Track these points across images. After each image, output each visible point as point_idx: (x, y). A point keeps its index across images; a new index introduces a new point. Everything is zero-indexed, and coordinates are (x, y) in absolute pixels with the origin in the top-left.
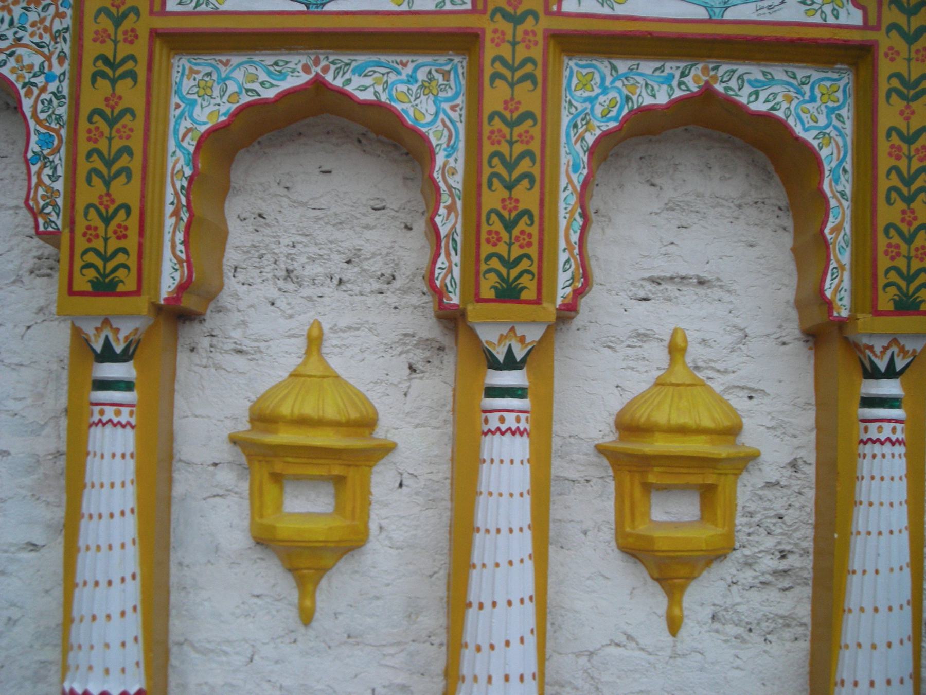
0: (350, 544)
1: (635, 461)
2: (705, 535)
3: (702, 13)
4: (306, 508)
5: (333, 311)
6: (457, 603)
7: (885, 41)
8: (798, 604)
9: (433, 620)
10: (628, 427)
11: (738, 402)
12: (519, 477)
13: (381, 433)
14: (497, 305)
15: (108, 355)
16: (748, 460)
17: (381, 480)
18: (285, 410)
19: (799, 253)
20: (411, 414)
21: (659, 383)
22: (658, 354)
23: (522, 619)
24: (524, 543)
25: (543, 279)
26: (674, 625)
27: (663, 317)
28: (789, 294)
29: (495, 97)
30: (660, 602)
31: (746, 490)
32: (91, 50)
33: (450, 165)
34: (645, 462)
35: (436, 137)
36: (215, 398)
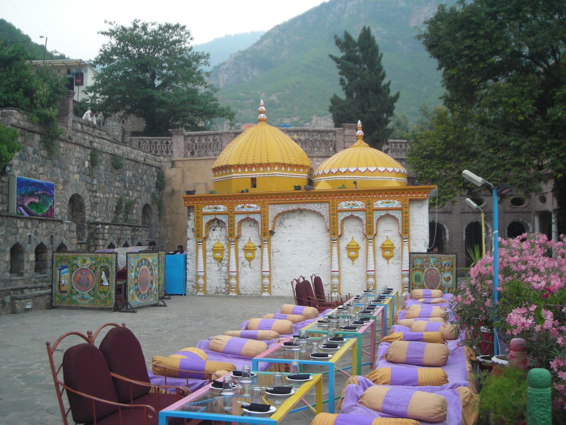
0: (357, 257)
1: (384, 248)
4: (353, 254)
5: (354, 235)
6: (367, 262)
9: (365, 264)
10: (383, 245)
12: (372, 250)
14: (370, 233)
17: (360, 251)
22: (385, 238)
23: (373, 262)
24: (372, 256)
25: (373, 232)
26: (388, 264)
27: (386, 234)
30: (387, 261)
31: (395, 250)
33: (364, 222)
36: (344, 244)
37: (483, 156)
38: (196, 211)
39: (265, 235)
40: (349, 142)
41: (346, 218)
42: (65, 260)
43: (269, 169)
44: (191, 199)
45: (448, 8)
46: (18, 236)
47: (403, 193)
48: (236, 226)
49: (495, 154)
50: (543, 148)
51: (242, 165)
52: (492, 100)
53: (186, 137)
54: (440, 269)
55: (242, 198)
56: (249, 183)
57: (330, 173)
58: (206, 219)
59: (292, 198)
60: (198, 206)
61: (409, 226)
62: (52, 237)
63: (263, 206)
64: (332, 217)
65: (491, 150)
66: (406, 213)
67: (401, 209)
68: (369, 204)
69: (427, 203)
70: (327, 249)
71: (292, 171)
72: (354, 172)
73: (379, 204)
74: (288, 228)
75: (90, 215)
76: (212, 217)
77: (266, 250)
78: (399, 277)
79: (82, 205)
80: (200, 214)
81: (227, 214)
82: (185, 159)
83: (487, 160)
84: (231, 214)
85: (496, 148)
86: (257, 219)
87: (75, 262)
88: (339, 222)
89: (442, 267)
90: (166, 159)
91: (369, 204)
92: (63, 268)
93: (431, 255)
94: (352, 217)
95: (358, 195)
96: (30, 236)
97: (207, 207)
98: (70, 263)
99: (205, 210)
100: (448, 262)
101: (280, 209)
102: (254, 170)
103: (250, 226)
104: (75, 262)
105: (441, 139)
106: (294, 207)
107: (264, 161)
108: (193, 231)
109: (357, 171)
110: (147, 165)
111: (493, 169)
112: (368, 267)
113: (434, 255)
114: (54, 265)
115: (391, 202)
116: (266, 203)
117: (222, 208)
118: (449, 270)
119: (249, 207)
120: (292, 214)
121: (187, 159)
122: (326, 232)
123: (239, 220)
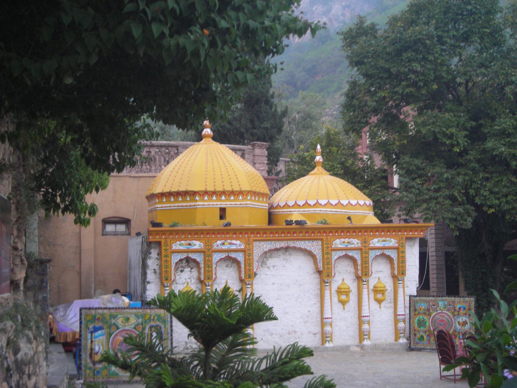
0: (348, 301)
1: (376, 291)
2: (383, 298)
3: (382, 245)
4: (343, 297)
5: (345, 276)
7: (400, 247)
8: (392, 305)
9: (357, 309)
10: (375, 287)
11: (385, 284)
13: (351, 289)
15: (328, 283)
16: (387, 290)
17: (351, 294)
18: (343, 287)
19: (391, 267)
20: (353, 286)
21: (377, 282)
26: (380, 308)
27: (377, 275)
28: (390, 272)
29: (364, 255)
30: (378, 305)
31: (386, 293)
32: (325, 251)
33: (359, 262)
34: (377, 291)
35: (358, 259)
36: (335, 287)
37: (413, 187)
38: (163, 248)
39: (250, 277)
40: (259, 163)
41: (340, 257)
42: (98, 319)
43: (241, 198)
44: (157, 233)
45: (368, 23)
47: (400, 231)
48: (214, 266)
49: (423, 184)
50: (474, 181)
51: (210, 191)
52: (432, 129)
54: (453, 313)
55: (223, 233)
56: (218, 214)
57: (306, 204)
58: (175, 258)
59: (281, 233)
60: (166, 241)
61: (405, 266)
63: (248, 243)
65: (418, 181)
66: (404, 252)
67: (397, 248)
68: (365, 242)
69: (418, 241)
70: (316, 292)
72: (336, 205)
73: (376, 242)
74: (271, 268)
76: (184, 256)
78: (391, 322)
80: (170, 251)
81: (204, 252)
83: (417, 191)
84: (207, 253)
85: (423, 179)
86: (239, 259)
87: (113, 321)
88: (333, 262)
89: (455, 310)
91: (365, 242)
92: (96, 330)
93: (440, 298)
94: (346, 257)
95: (354, 232)
97: (178, 242)
98: (107, 323)
99: (176, 246)
100: (466, 305)
101: (267, 246)
102: (223, 198)
103: (227, 266)
104: (113, 321)
105: (338, 164)
106: (283, 244)
107: (236, 188)
108: (155, 272)
109: (339, 205)
111: (425, 201)
112: (363, 312)
113: (444, 298)
114: (83, 326)
115: (388, 241)
116: (251, 239)
117: (197, 245)
118: (466, 314)
119: (230, 244)
120: (276, 252)
122: (314, 273)
123: (218, 259)
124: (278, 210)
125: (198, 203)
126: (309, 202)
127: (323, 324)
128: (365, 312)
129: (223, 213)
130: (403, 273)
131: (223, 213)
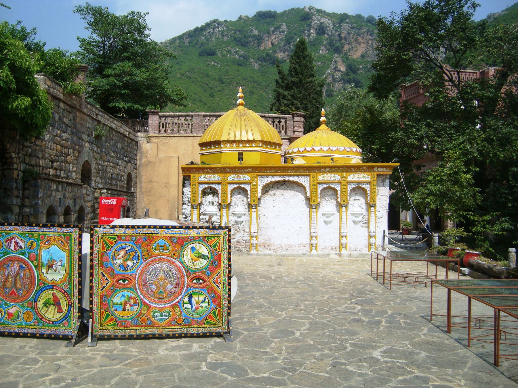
38: (192, 179)
41: (324, 189)
46: (52, 198)
53: (160, 117)
62: (75, 200)
64: (312, 187)
71: (271, 148)
75: (95, 182)
77: (254, 214)
79: (90, 171)
82: (159, 135)
90: (143, 135)
96: (60, 198)
102: (241, 145)
110: (131, 139)
121: (161, 135)
124: (288, 156)
125: (222, 149)
126: (307, 149)
127: (312, 237)
128: (344, 229)
129: (240, 156)
130: (374, 201)
131: (240, 156)
